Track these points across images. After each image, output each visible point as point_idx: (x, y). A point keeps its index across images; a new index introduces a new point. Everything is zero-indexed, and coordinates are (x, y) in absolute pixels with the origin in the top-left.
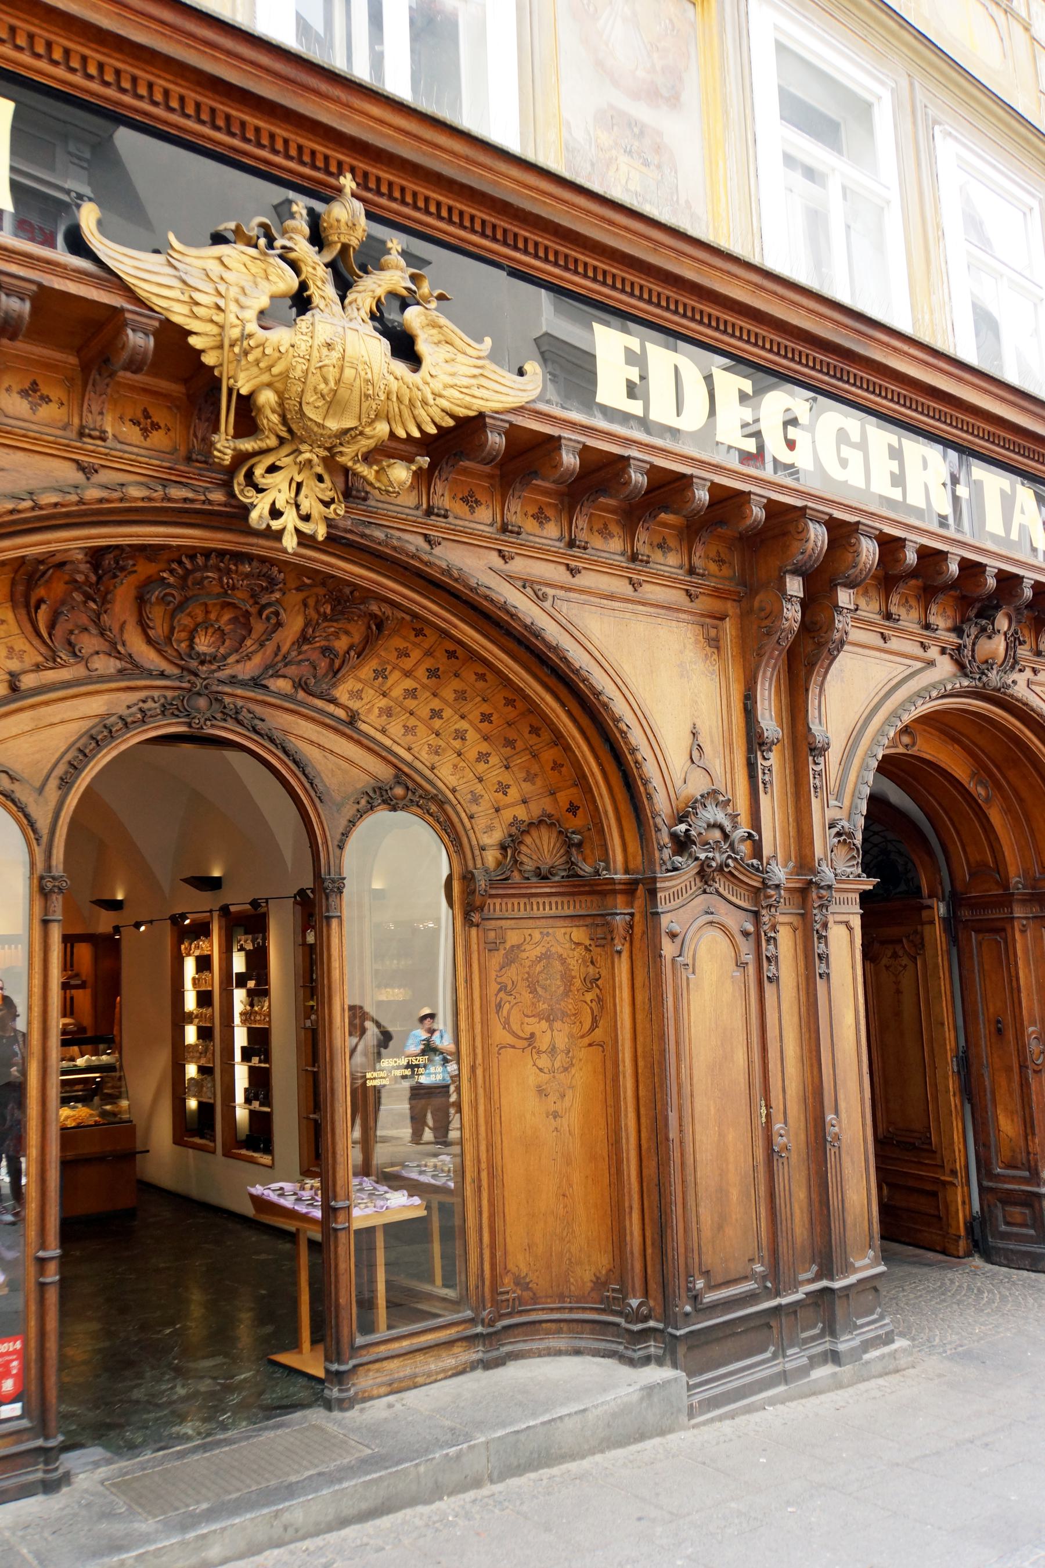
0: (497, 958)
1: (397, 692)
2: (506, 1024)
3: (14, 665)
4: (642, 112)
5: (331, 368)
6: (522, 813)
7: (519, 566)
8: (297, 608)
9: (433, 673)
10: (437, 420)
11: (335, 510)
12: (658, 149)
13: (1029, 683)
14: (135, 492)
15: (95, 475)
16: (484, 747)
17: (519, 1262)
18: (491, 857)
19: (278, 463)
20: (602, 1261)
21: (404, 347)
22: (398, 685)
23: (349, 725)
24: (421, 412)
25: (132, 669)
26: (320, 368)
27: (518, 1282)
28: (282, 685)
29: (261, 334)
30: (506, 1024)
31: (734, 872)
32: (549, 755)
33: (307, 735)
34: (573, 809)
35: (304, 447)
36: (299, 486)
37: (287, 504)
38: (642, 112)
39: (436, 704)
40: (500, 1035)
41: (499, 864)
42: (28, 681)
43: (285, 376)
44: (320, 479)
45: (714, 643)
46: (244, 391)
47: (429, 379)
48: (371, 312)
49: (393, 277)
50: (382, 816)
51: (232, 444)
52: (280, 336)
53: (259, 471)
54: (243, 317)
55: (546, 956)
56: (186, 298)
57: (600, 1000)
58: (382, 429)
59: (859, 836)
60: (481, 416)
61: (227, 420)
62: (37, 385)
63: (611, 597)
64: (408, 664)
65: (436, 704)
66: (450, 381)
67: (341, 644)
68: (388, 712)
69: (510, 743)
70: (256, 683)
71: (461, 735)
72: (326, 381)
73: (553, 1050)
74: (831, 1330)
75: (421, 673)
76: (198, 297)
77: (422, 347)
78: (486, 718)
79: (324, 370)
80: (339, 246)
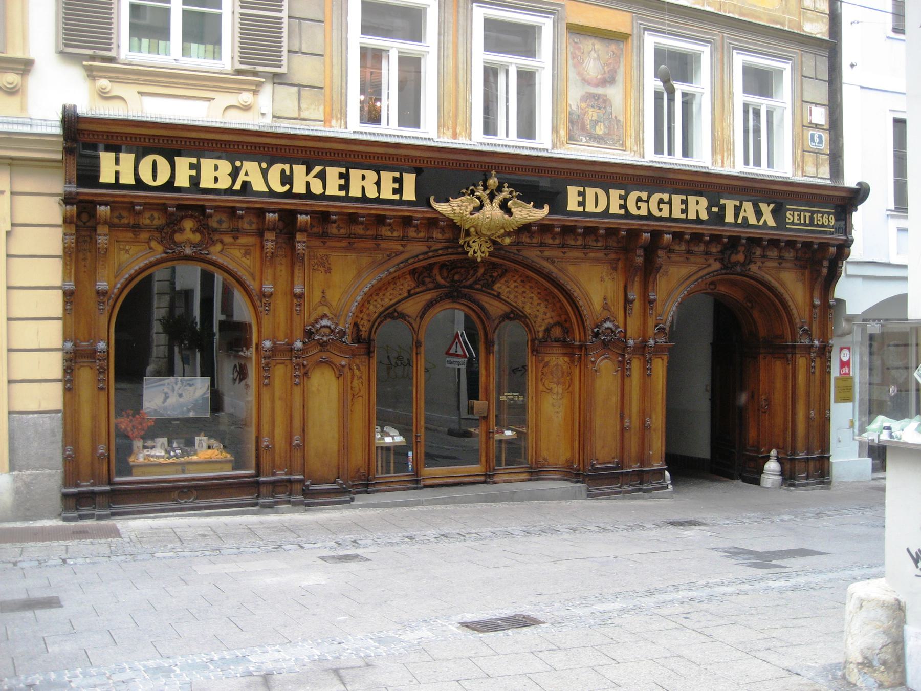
0: (542, 365)
1: (512, 286)
2: (544, 385)
4: (600, 91)
7: (547, 253)
9: (522, 281)
12: (605, 101)
13: (760, 267)
16: (539, 301)
17: (545, 453)
18: (541, 335)
20: (568, 455)
21: (508, 212)
22: (513, 285)
23: (498, 297)
25: (438, 286)
28: (478, 286)
30: (544, 385)
31: (614, 344)
32: (558, 305)
33: (485, 300)
34: (566, 321)
37: (478, 250)
38: (600, 91)
39: (523, 289)
40: (541, 387)
41: (544, 338)
42: (412, 292)
45: (615, 269)
50: (507, 322)
52: (477, 215)
55: (557, 365)
57: (571, 379)
58: (502, 231)
59: (667, 328)
61: (462, 235)
63: (577, 258)
64: (515, 279)
65: (523, 289)
67: (495, 274)
68: (509, 292)
69: (546, 300)
70: (471, 287)
73: (557, 393)
74: (641, 483)
75: (519, 281)
77: (513, 210)
78: (539, 293)
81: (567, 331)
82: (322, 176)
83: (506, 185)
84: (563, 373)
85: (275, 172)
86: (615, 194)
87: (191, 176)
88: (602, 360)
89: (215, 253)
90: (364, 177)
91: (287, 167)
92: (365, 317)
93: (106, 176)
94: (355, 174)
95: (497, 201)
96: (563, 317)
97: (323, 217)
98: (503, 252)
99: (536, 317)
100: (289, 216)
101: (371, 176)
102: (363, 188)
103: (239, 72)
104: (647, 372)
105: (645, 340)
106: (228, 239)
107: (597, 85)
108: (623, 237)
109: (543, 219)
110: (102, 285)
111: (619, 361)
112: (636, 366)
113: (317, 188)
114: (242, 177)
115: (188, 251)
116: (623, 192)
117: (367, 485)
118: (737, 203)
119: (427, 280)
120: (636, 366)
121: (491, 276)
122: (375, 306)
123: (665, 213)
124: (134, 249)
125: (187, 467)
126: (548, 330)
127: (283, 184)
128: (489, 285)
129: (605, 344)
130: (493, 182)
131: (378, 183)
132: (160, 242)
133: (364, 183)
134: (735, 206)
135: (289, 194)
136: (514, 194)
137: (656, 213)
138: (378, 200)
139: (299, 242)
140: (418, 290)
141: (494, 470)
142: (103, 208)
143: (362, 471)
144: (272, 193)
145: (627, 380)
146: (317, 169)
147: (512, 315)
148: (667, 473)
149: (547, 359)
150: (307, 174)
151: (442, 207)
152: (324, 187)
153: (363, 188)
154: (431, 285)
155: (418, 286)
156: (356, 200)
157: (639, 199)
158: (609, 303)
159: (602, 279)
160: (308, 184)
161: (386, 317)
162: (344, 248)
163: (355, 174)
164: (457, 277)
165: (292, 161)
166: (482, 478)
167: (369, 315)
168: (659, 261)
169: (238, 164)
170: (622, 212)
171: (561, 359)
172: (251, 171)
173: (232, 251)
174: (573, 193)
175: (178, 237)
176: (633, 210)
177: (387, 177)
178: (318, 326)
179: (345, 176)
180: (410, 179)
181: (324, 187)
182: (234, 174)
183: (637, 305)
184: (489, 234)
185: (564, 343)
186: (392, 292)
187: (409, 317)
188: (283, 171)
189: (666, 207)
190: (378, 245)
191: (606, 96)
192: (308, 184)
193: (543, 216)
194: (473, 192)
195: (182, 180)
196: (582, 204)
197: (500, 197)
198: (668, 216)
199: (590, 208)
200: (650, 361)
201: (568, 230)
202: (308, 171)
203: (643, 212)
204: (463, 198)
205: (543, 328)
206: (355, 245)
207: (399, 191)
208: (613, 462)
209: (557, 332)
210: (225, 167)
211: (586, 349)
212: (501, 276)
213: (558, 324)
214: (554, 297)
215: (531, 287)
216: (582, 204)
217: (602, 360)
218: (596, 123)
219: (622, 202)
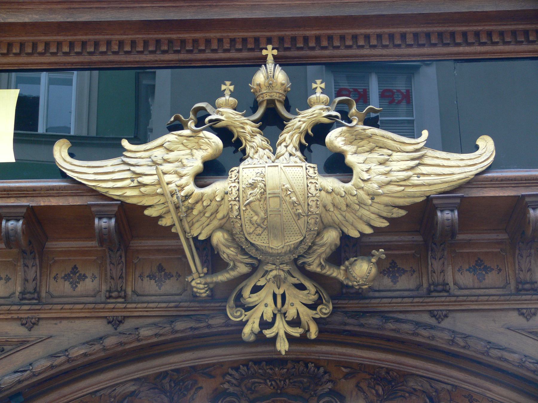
5: (257, 203)
8: (354, 393)
10: (385, 214)
11: (321, 310)
14: (144, 332)
15: (121, 325)
19: (259, 284)
24: (364, 212)
26: (248, 204)
29: (198, 191)
35: (269, 267)
36: (283, 296)
43: (227, 217)
44: (301, 287)
46: (201, 238)
47: (362, 184)
48: (300, 144)
51: (203, 281)
52: (218, 187)
53: (246, 293)
56: (135, 184)
58: (331, 237)
60: (429, 199)
62: (77, 268)
66: (383, 178)
72: (257, 214)
76: (145, 180)
77: (350, 159)
79: (253, 205)
80: (265, 104)
95: (290, 138)
98: (374, 321)
151: (87, 171)
193: (475, 170)
197: (300, 122)
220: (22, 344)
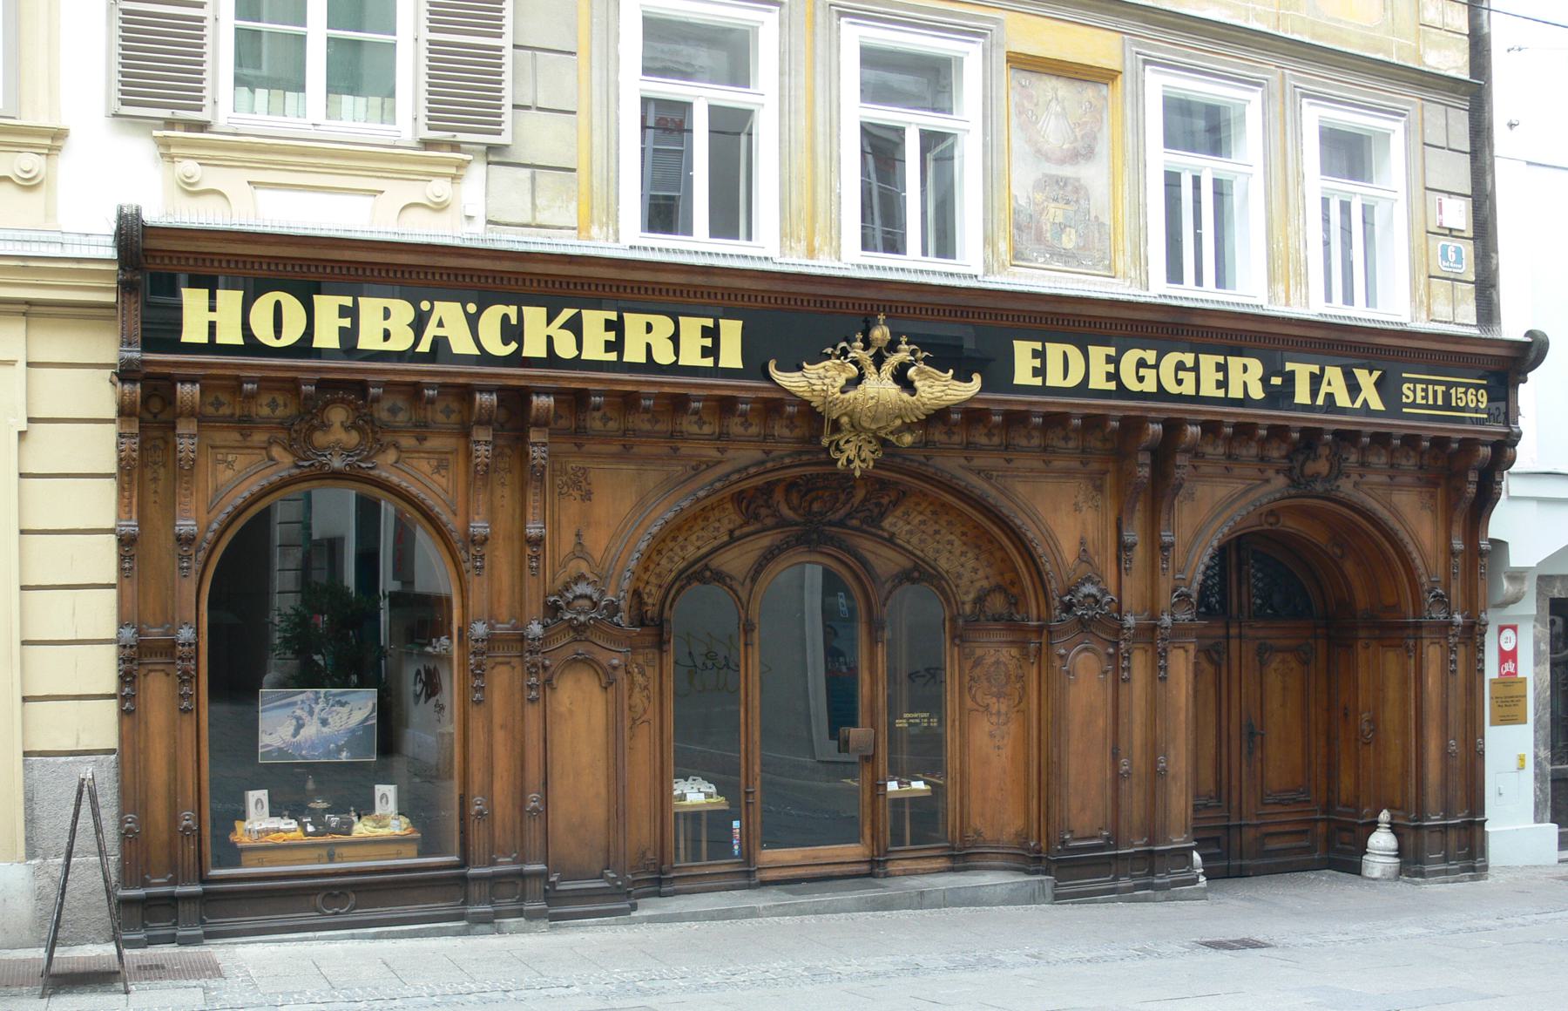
0: (969, 663)
1: (916, 522)
2: (974, 698)
3: (731, 526)
4: (1067, 171)
6: (985, 583)
7: (978, 462)
9: (934, 513)
12: (1076, 190)
13: (1356, 484)
16: (964, 548)
17: (976, 822)
18: (968, 608)
20: (1019, 823)
23: (890, 541)
25: (782, 523)
27: (976, 831)
28: (855, 522)
30: (974, 698)
32: (998, 555)
33: (867, 546)
34: (1012, 583)
37: (855, 455)
39: (937, 527)
40: (969, 703)
41: (973, 612)
42: (737, 533)
45: (1099, 489)
49: (903, 355)
50: (907, 585)
52: (851, 394)
54: (835, 392)
55: (997, 662)
57: (1023, 688)
58: (898, 422)
59: (1195, 595)
61: (827, 429)
63: (1032, 470)
64: (920, 509)
65: (937, 527)
68: (911, 532)
69: (978, 547)
70: (841, 523)
71: (951, 543)
73: (999, 713)
74: (1152, 873)
75: (928, 512)
77: (917, 384)
78: (964, 534)
81: (1015, 601)
82: (575, 326)
83: (904, 339)
84: (1008, 677)
85: (491, 319)
86: (1098, 353)
87: (341, 329)
88: (1079, 652)
89: (386, 466)
90: (649, 328)
91: (512, 311)
92: (653, 580)
93: (194, 331)
94: (634, 323)
95: (887, 368)
96: (1008, 576)
97: (575, 400)
98: (899, 460)
99: (959, 576)
100: (515, 399)
101: (663, 324)
102: (649, 347)
103: (427, 144)
104: (1159, 673)
105: (1154, 616)
106: (407, 442)
107: (1062, 162)
108: (1113, 431)
109: (972, 399)
110: (186, 525)
111: (1110, 655)
112: (1139, 663)
113: (566, 347)
114: (431, 331)
115: (337, 463)
116: (1112, 351)
117: (659, 882)
118: (1316, 369)
119: (763, 511)
120: (1139, 663)
121: (878, 505)
122: (671, 560)
123: (1188, 389)
124: (241, 461)
125: (338, 851)
126: (980, 600)
127: (506, 342)
128: (875, 520)
129: (1084, 625)
130: (881, 333)
131: (675, 339)
132: (288, 448)
133: (650, 338)
134: (1312, 375)
135: (517, 359)
136: (919, 355)
137: (1172, 388)
138: (675, 368)
139: (534, 444)
140: (746, 529)
141: (887, 852)
142: (188, 387)
143: (650, 855)
144: (485, 358)
145: (1123, 688)
146: (567, 313)
147: (916, 574)
148: (1196, 856)
149: (979, 652)
150: (548, 323)
151: (789, 381)
152: (579, 346)
153: (649, 347)
154: (769, 521)
155: (747, 523)
156: (633, 367)
157: (1142, 363)
158: (1091, 550)
159: (1077, 508)
160: (550, 340)
161: (689, 580)
162: (613, 456)
163: (634, 323)
164: (816, 507)
165: (521, 300)
166: (865, 868)
167: (659, 575)
168: (1178, 473)
169: (425, 306)
170: (1112, 386)
171: (1004, 651)
172: (449, 320)
173: (415, 462)
174: (1023, 350)
175: (320, 438)
176: (1131, 384)
177: (691, 327)
178: (570, 596)
179: (616, 326)
180: (731, 332)
181: (579, 346)
182: (419, 325)
183: (1139, 555)
184: (874, 427)
185: (1012, 624)
186: (700, 534)
187: (732, 578)
188: (505, 318)
189: (1189, 378)
190: (676, 450)
191: (1078, 180)
192: (550, 340)
193: (970, 394)
194: (845, 352)
195: (327, 337)
196: (1040, 372)
197: (893, 360)
198: (1193, 393)
199: (1054, 379)
200: (1163, 655)
201: (1016, 419)
202: (549, 322)
203: (1150, 386)
204: (827, 363)
205: (972, 596)
206: (635, 450)
207: (712, 351)
208: (1101, 837)
209: (997, 603)
210: (403, 311)
211: (1050, 632)
212: (895, 504)
213: (999, 588)
214: (992, 540)
215: (949, 523)
216: (1040, 372)
217: (1079, 652)
218: (1062, 228)
219: (1111, 368)
220: (719, 462)
